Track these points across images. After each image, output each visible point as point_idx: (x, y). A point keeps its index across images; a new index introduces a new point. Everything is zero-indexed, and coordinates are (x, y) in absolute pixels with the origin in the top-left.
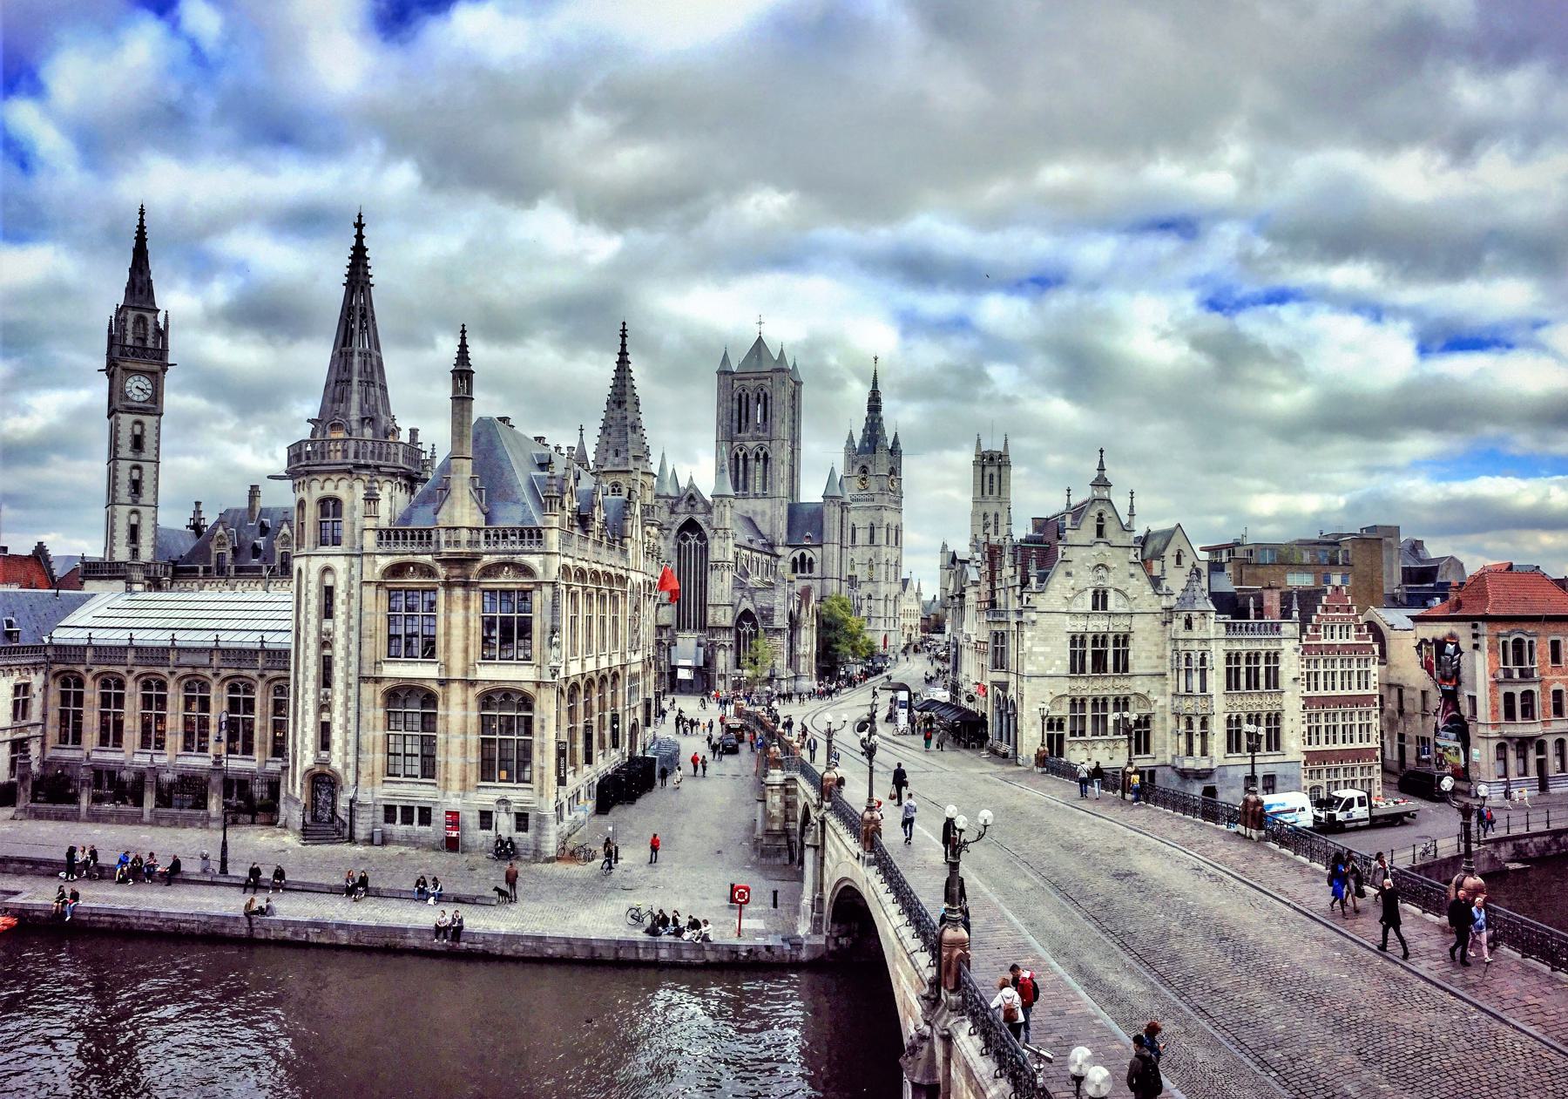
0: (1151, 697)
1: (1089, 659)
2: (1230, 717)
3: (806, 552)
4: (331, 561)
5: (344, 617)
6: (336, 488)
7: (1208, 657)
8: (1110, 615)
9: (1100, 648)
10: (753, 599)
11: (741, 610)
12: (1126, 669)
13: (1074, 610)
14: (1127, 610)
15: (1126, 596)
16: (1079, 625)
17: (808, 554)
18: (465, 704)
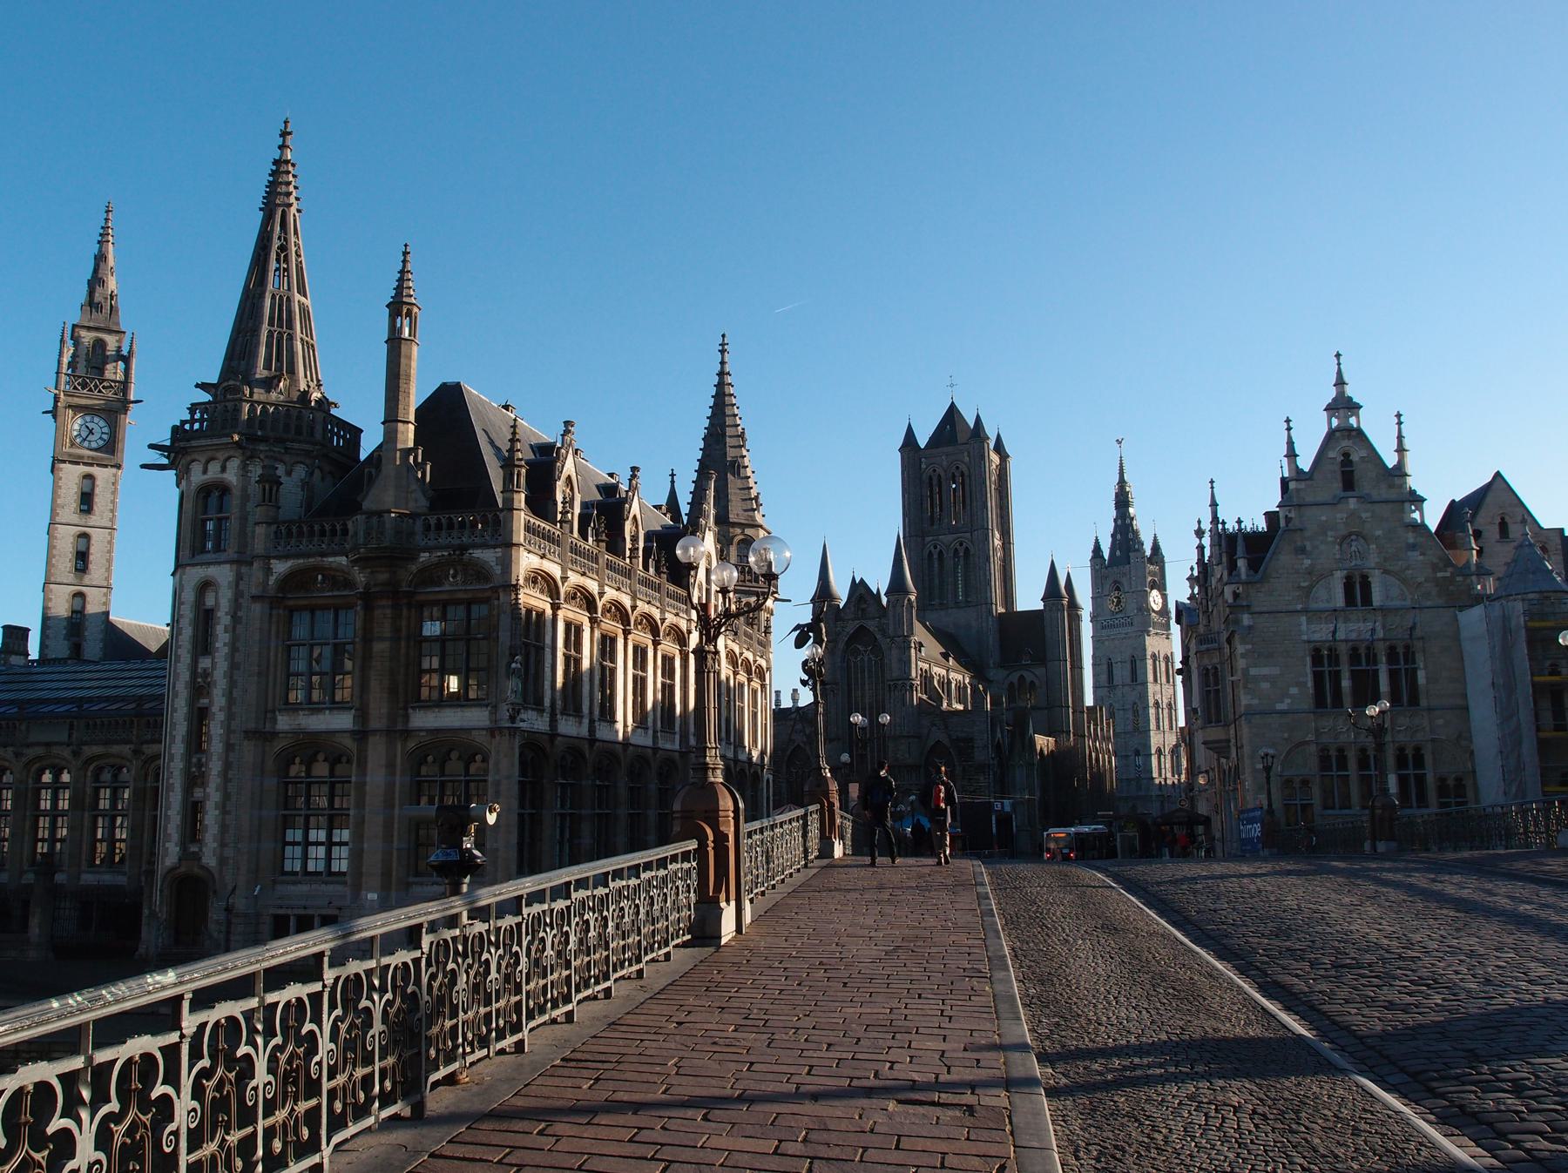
1: (1346, 683)
3: (1025, 674)
4: (212, 571)
5: (226, 650)
6: (224, 469)
8: (1383, 610)
10: (946, 727)
11: (931, 743)
12: (1414, 700)
13: (1314, 606)
15: (1404, 581)
17: (1029, 677)
18: (390, 765)
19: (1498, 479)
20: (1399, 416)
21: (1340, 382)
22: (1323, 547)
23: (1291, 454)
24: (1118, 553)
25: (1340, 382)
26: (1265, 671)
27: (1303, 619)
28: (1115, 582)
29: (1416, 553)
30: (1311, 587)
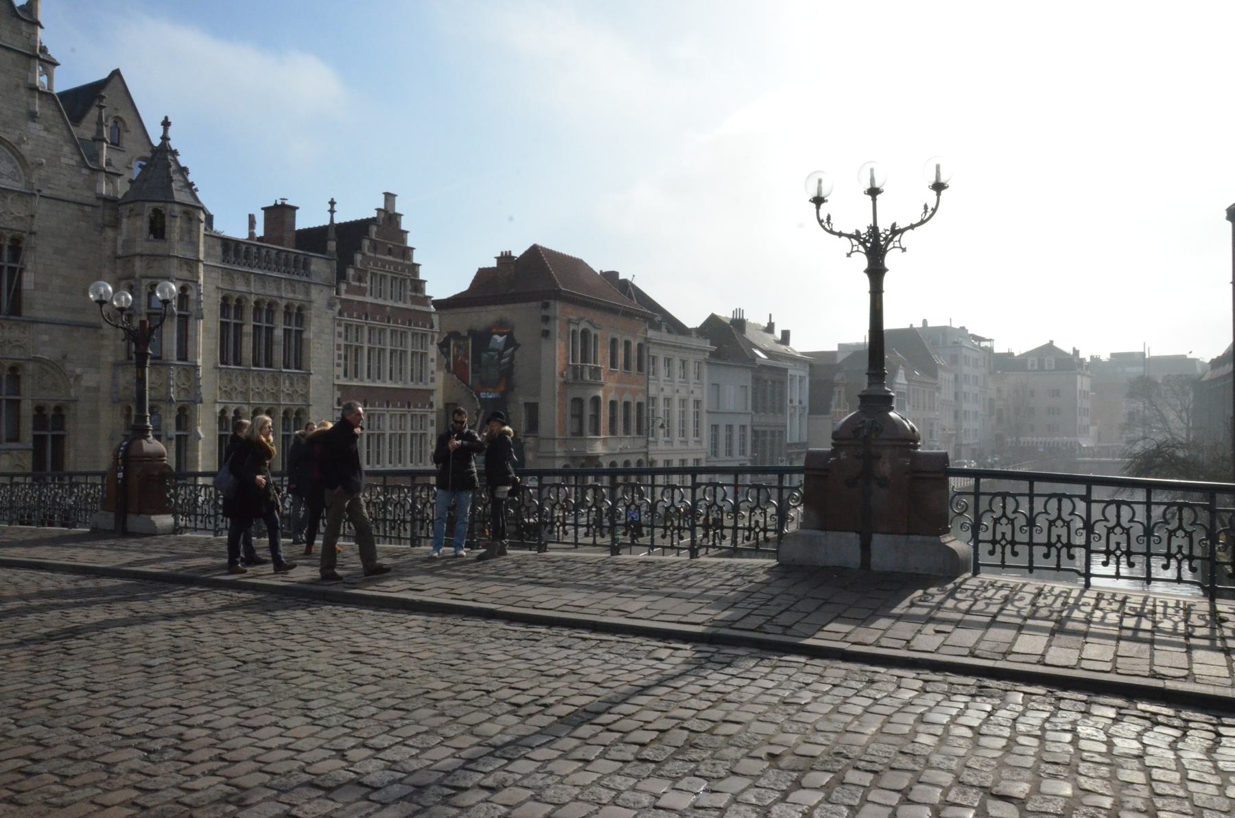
0: (69, 367)
2: (223, 412)
7: (192, 295)
14: (19, 186)
19: (116, 77)
29: (38, 126)
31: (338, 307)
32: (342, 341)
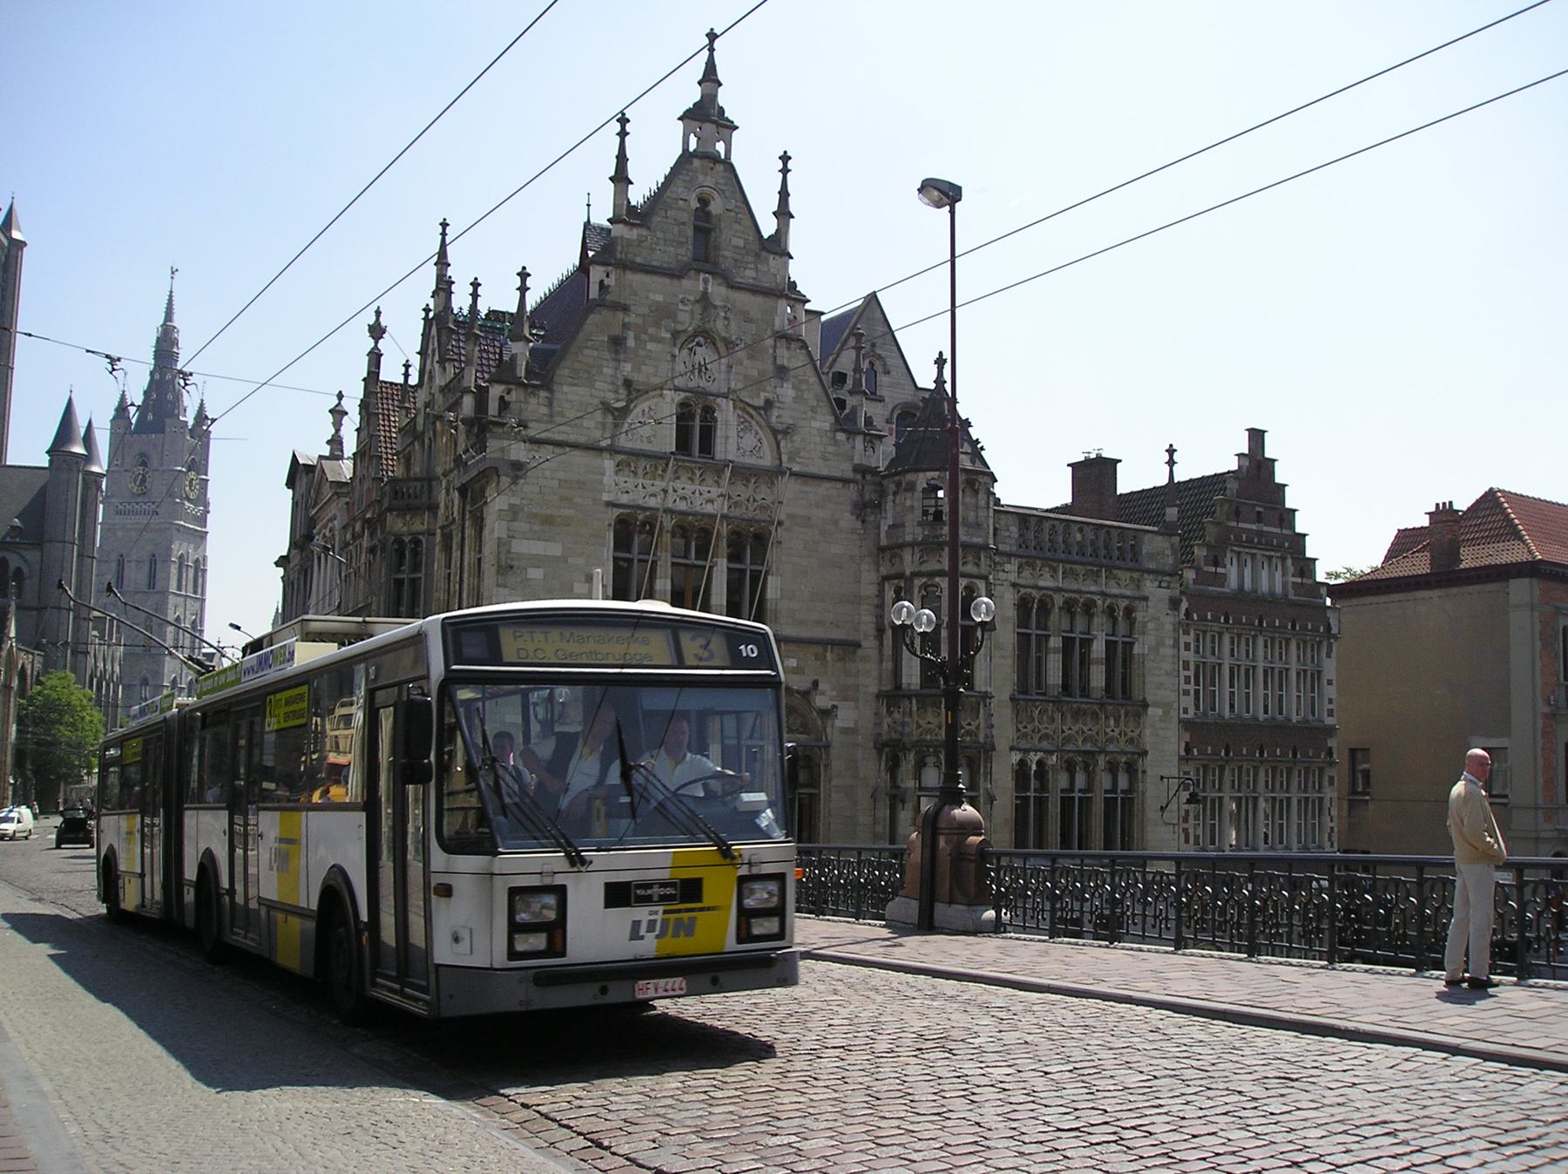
2: (1022, 763)
9: (692, 560)
13: (624, 442)
16: (644, 492)
20: (785, 158)
21: (710, 77)
22: (650, 346)
23: (621, 178)
24: (150, 417)
25: (710, 77)
26: (537, 548)
27: (609, 464)
28: (142, 455)
30: (624, 412)
31: (1184, 605)
32: (1190, 656)
